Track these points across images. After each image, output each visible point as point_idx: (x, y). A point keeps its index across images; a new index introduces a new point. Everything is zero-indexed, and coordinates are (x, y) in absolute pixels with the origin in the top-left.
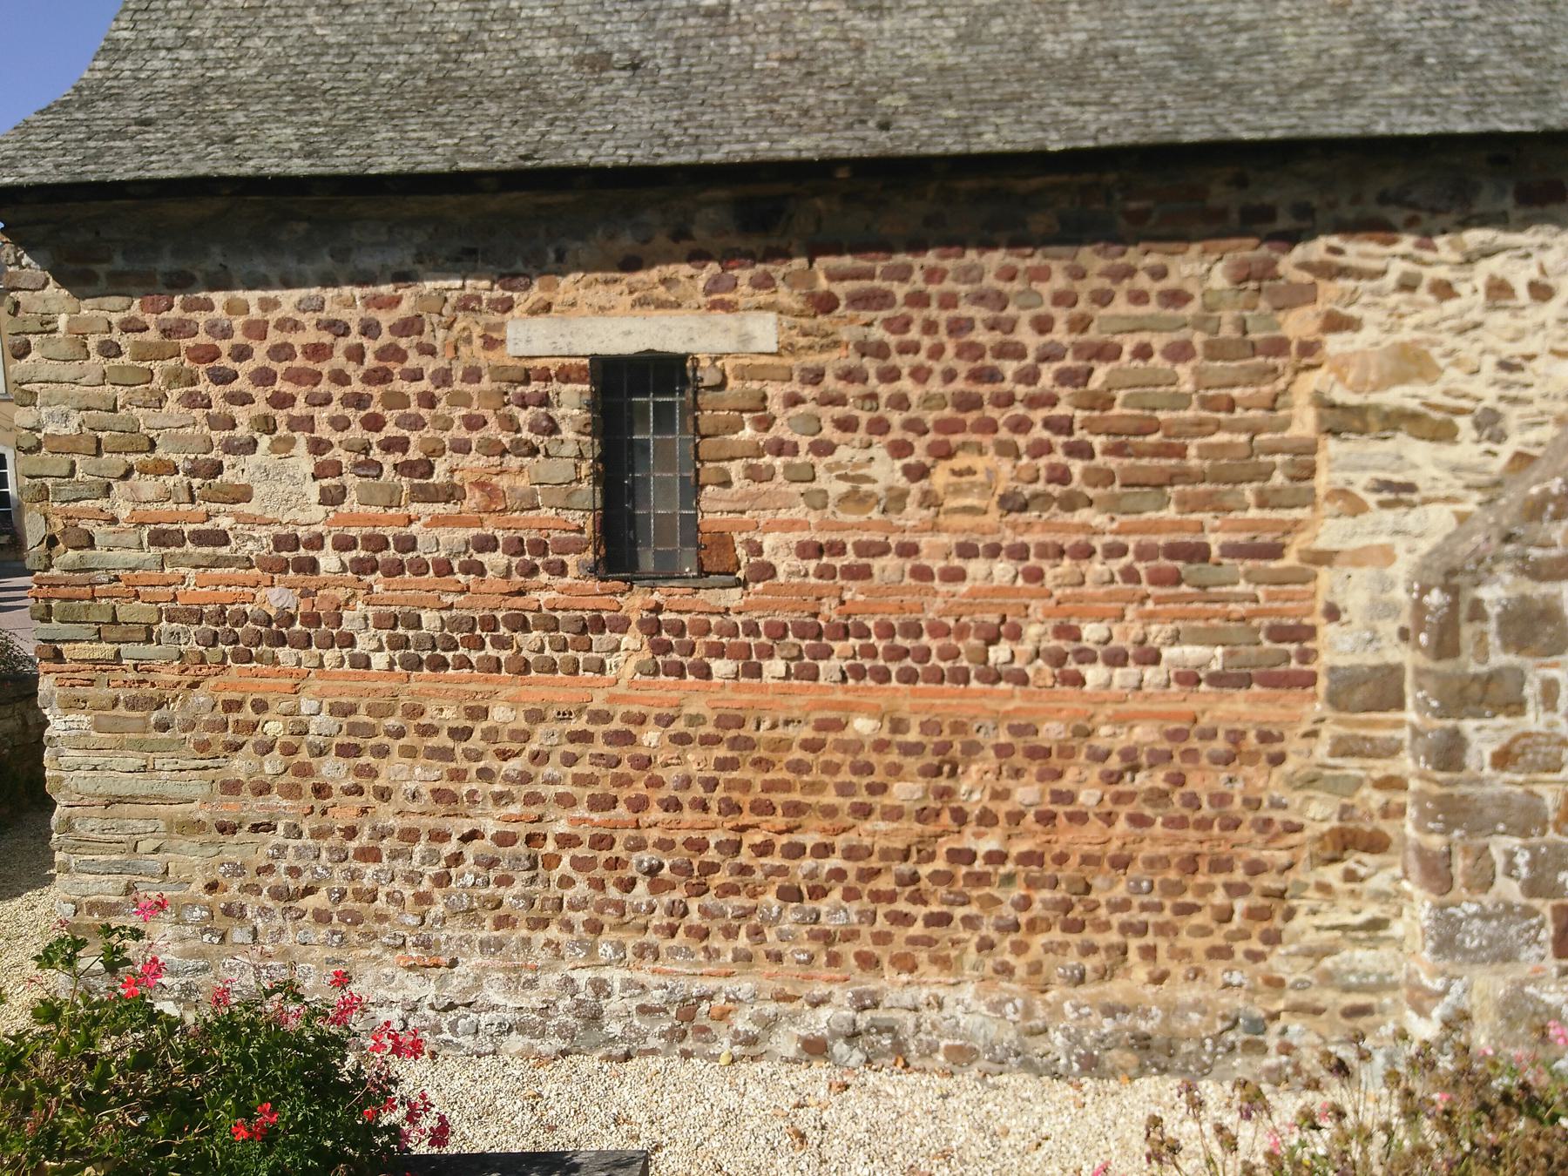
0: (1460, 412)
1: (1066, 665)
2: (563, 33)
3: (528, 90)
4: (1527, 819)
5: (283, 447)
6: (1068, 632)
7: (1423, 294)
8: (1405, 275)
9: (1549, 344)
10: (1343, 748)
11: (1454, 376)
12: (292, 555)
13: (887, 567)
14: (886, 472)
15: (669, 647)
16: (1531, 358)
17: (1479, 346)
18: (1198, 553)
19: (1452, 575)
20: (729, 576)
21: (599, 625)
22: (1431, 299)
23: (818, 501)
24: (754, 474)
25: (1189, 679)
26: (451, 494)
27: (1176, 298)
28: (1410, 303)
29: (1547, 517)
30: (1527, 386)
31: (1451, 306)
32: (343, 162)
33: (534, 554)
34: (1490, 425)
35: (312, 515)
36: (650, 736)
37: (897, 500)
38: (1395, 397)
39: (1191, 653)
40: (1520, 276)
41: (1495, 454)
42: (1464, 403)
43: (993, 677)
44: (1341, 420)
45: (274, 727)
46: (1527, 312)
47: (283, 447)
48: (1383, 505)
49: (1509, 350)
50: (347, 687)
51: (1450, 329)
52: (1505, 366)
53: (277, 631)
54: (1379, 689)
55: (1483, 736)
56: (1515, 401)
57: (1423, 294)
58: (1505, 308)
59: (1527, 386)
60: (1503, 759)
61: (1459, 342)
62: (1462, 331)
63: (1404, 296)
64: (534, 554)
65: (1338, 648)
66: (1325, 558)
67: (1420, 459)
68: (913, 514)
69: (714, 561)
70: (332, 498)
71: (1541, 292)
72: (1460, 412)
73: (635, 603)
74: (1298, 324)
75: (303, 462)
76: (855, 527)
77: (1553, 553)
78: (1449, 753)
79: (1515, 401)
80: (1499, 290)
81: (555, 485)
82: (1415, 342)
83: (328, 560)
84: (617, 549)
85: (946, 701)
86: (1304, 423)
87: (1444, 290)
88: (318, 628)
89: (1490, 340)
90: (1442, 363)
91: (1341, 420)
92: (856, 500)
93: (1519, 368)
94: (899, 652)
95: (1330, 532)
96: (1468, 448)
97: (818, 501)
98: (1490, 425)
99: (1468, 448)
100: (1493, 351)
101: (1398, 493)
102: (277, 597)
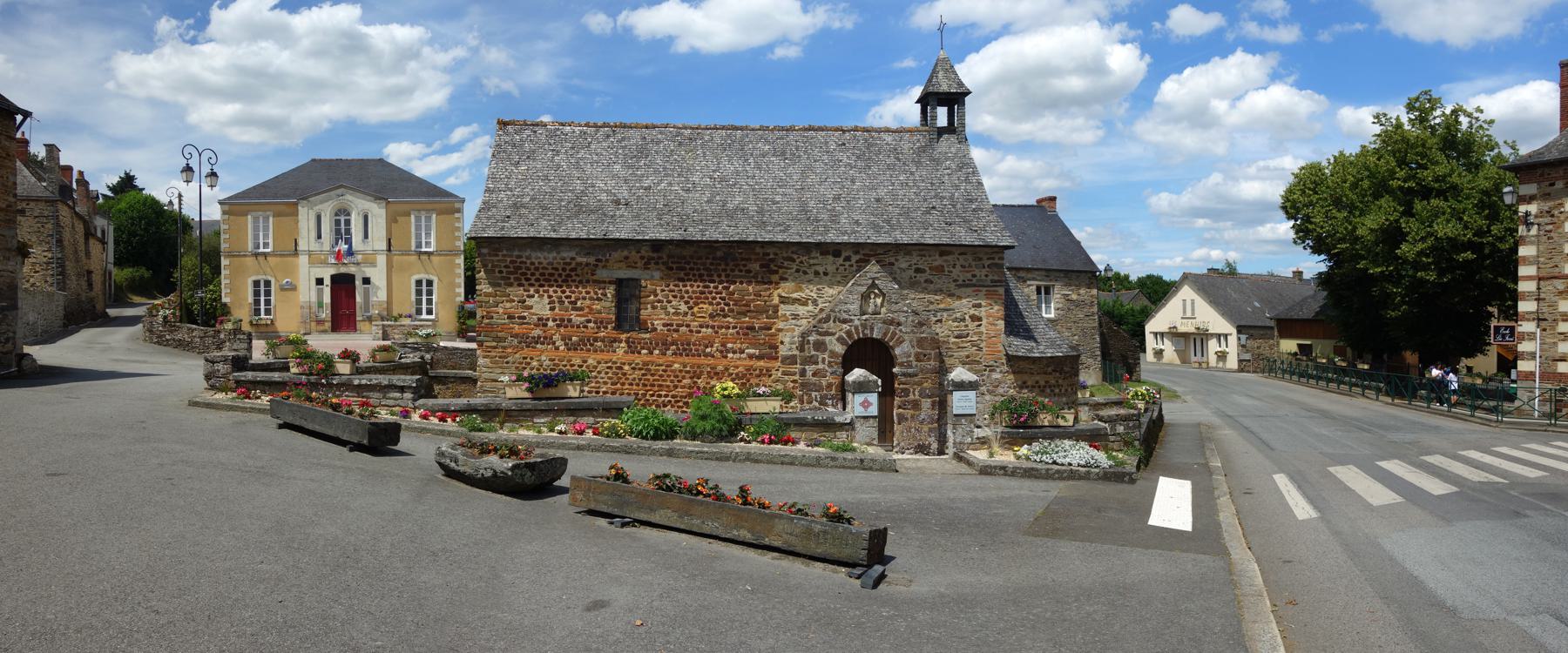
1: (724, 353)
2: (608, 192)
3: (598, 211)
4: (819, 388)
5: (541, 296)
6: (723, 345)
10: (784, 373)
12: (542, 322)
13: (683, 329)
14: (684, 308)
15: (632, 348)
18: (752, 328)
19: (804, 335)
20: (646, 330)
21: (615, 341)
23: (668, 314)
24: (654, 308)
25: (751, 357)
26: (581, 309)
27: (749, 271)
32: (562, 234)
33: (601, 324)
34: (815, 303)
35: (547, 313)
36: (626, 367)
37: (686, 314)
38: (795, 295)
39: (752, 351)
40: (821, 269)
43: (706, 355)
44: (784, 300)
45: (535, 363)
47: (541, 296)
50: (553, 354)
53: (537, 340)
54: (791, 360)
55: (810, 369)
60: (814, 375)
64: (601, 324)
65: (783, 351)
66: (780, 330)
67: (802, 310)
68: (689, 317)
69: (642, 326)
70: (552, 309)
71: (826, 274)
73: (624, 337)
74: (775, 278)
75: (546, 300)
76: (676, 320)
78: (803, 373)
80: (817, 273)
81: (606, 304)
83: (550, 323)
84: (619, 326)
85: (696, 360)
86: (776, 300)
87: (805, 273)
88: (548, 340)
91: (784, 300)
92: (676, 314)
94: (685, 349)
95: (781, 325)
96: (810, 308)
97: (668, 314)
98: (815, 303)
99: (810, 308)
101: (796, 317)
102: (537, 332)
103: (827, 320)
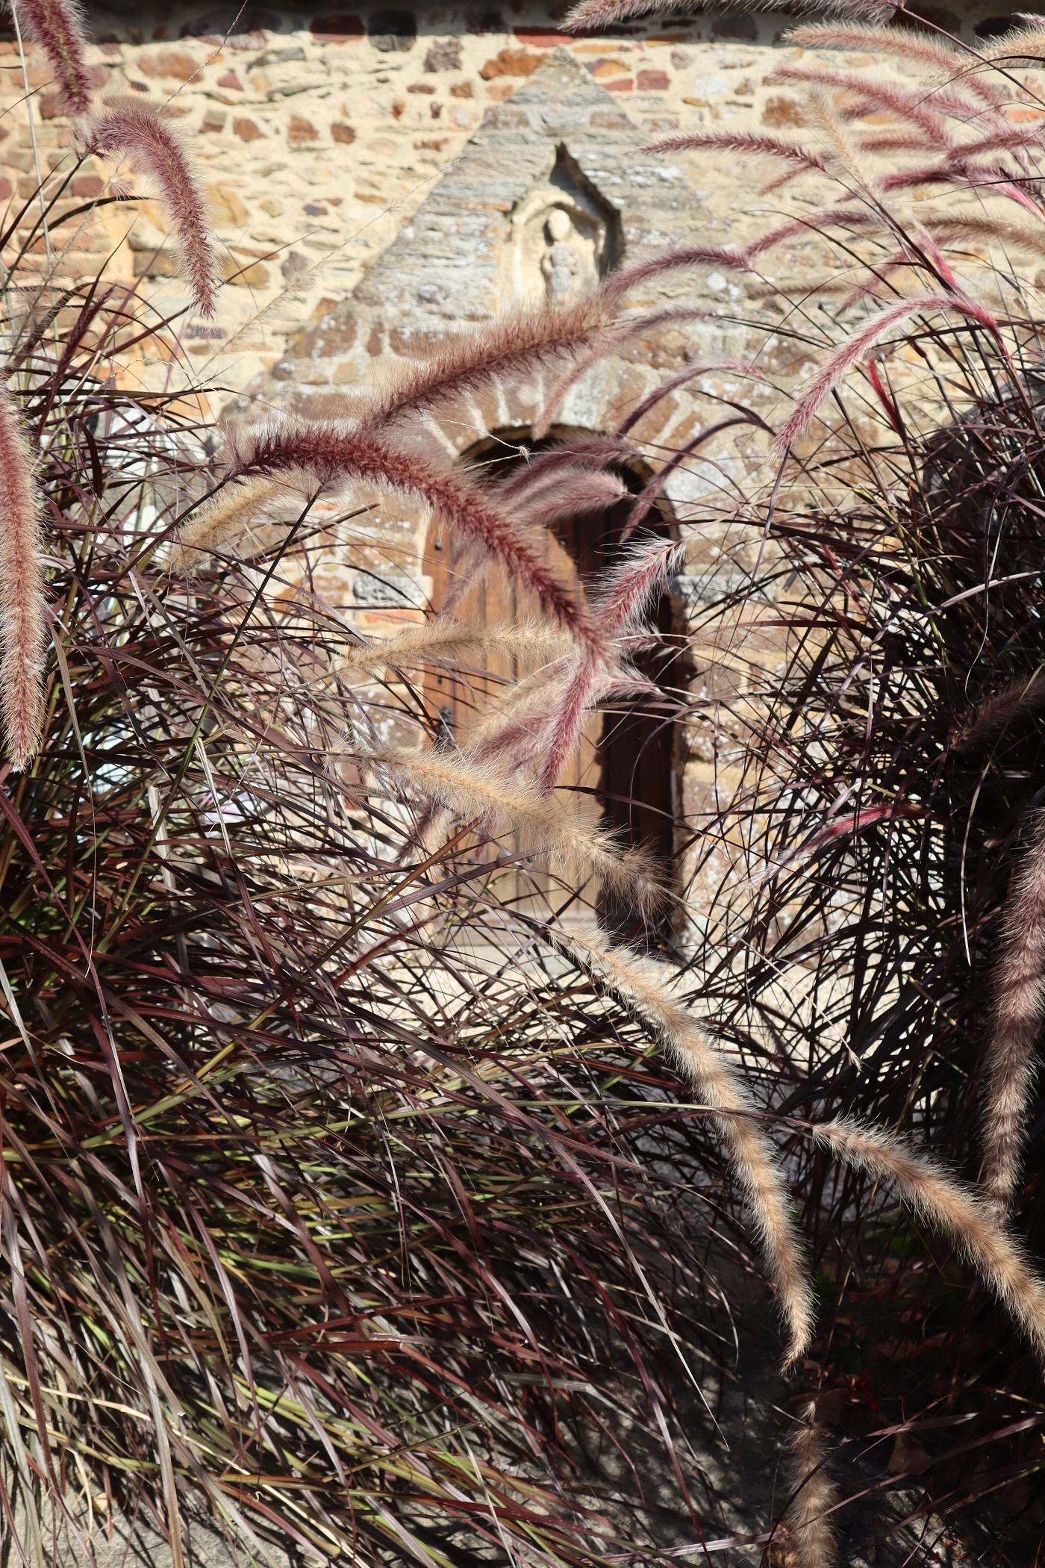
0: (269, 256)
7: (228, 134)
8: (210, 113)
9: (353, 188)
11: (259, 221)
16: (336, 202)
17: (284, 188)
22: (237, 139)
28: (214, 144)
29: (315, 353)
30: (336, 231)
31: (257, 144)
40: (321, 114)
41: (303, 301)
42: (270, 248)
46: (331, 154)
48: (197, 351)
49: (316, 194)
51: (255, 172)
52: (312, 210)
56: (320, 246)
57: (228, 134)
58: (310, 150)
59: (336, 231)
61: (263, 184)
62: (267, 173)
63: (212, 135)
71: (344, 134)
72: (269, 256)
77: (325, 390)
79: (320, 246)
80: (302, 131)
82: (221, 183)
87: (247, 131)
89: (300, 186)
90: (252, 206)
93: (324, 212)
100: (302, 197)
103: (341, 337)
